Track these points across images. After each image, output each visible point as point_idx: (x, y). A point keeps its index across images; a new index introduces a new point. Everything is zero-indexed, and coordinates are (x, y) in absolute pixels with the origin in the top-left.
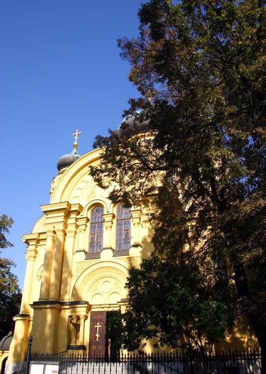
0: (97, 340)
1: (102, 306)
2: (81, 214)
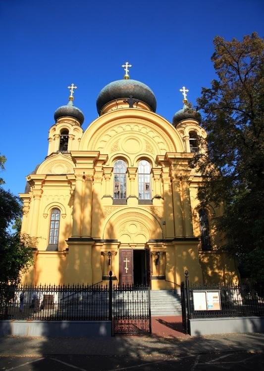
0: (127, 272)
1: (131, 245)
2: (107, 164)
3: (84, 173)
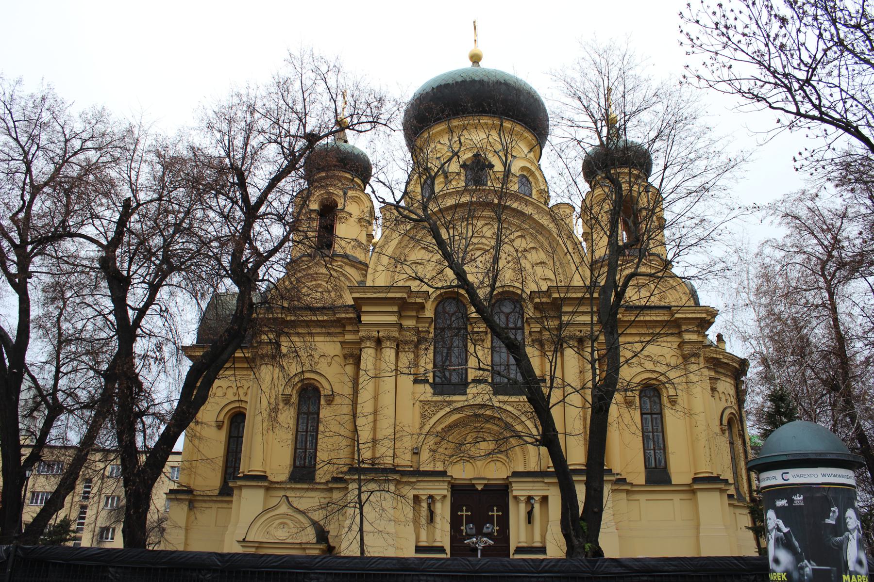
3: (378, 332)
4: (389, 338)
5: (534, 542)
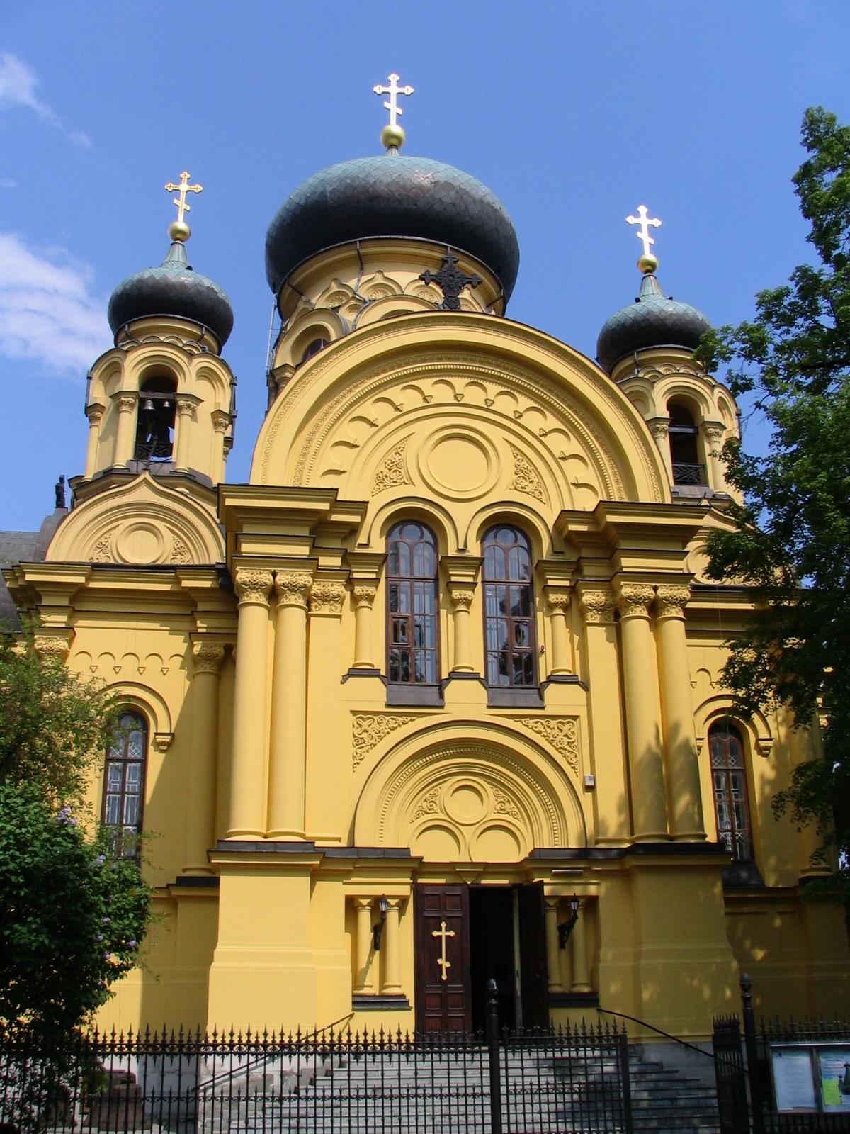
0: (444, 977)
3: (274, 575)
4: (294, 588)
5: (574, 985)
